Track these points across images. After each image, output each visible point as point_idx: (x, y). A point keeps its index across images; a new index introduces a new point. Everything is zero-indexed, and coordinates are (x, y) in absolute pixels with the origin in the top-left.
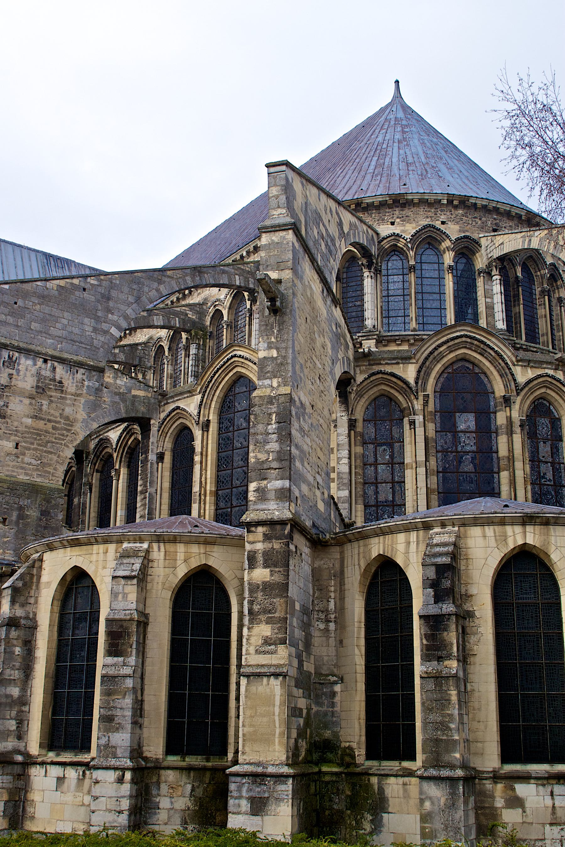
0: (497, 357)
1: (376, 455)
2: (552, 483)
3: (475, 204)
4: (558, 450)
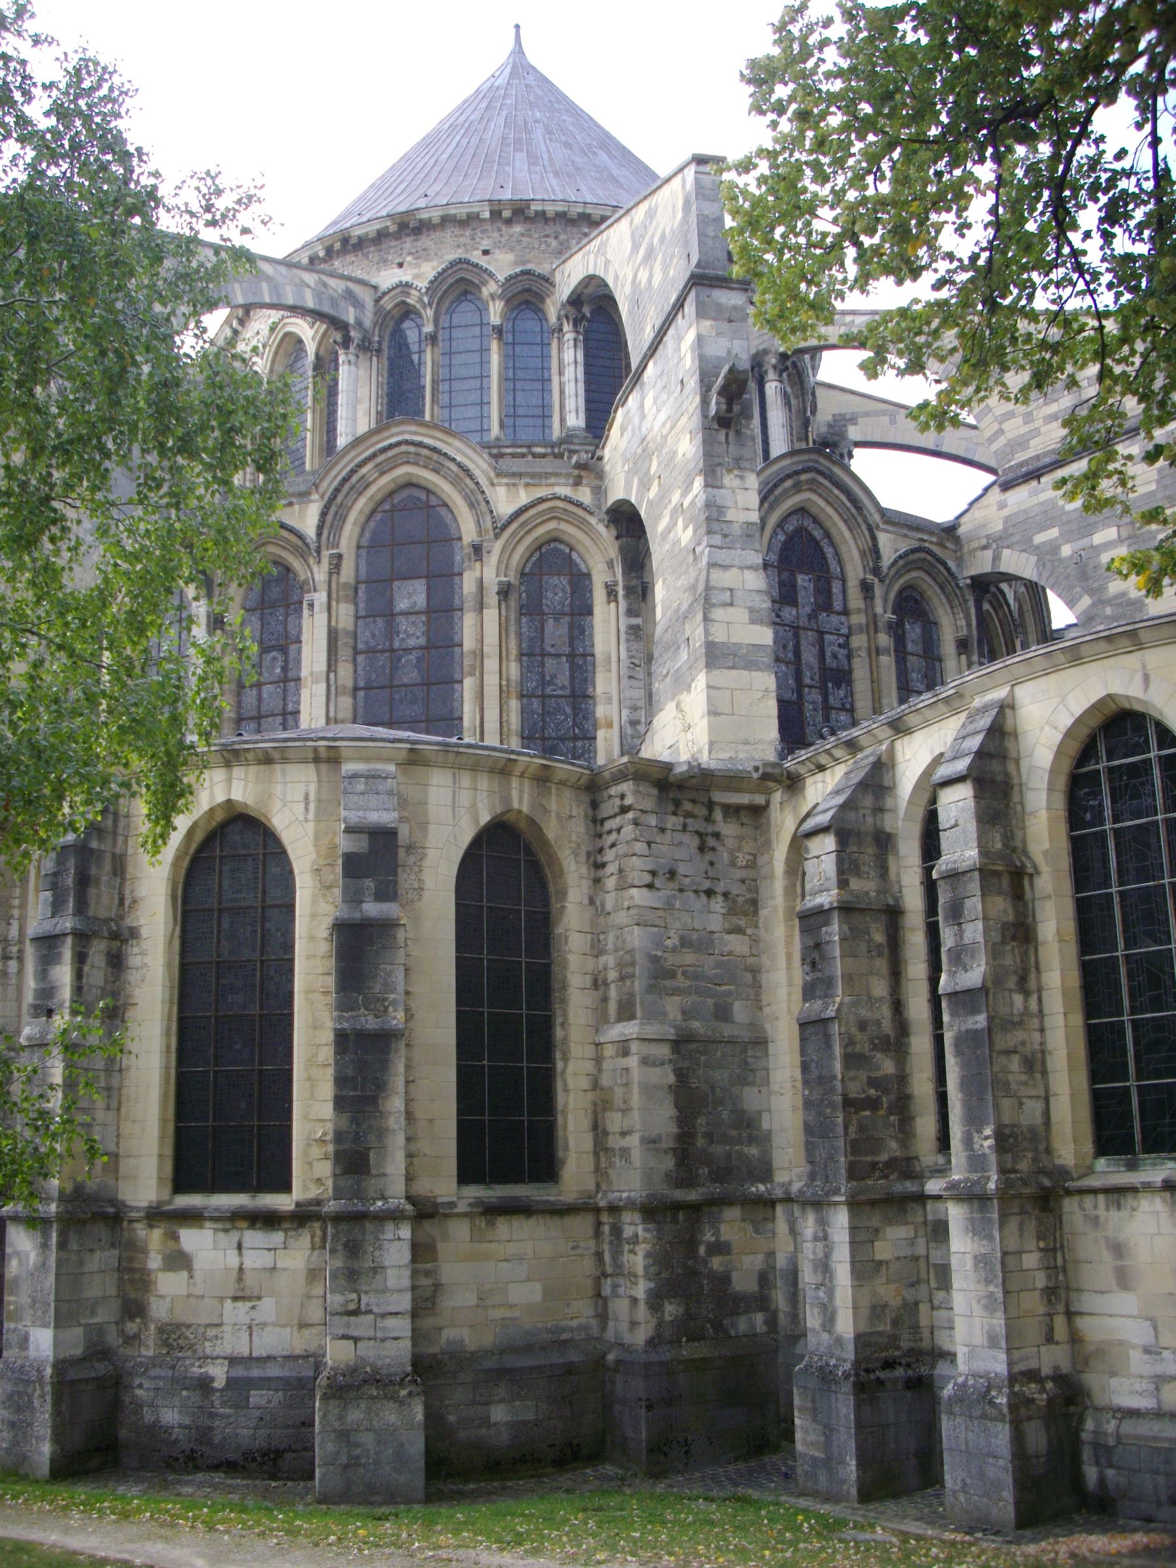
0: (462, 474)
2: (568, 692)
3: (544, 212)
4: (583, 632)
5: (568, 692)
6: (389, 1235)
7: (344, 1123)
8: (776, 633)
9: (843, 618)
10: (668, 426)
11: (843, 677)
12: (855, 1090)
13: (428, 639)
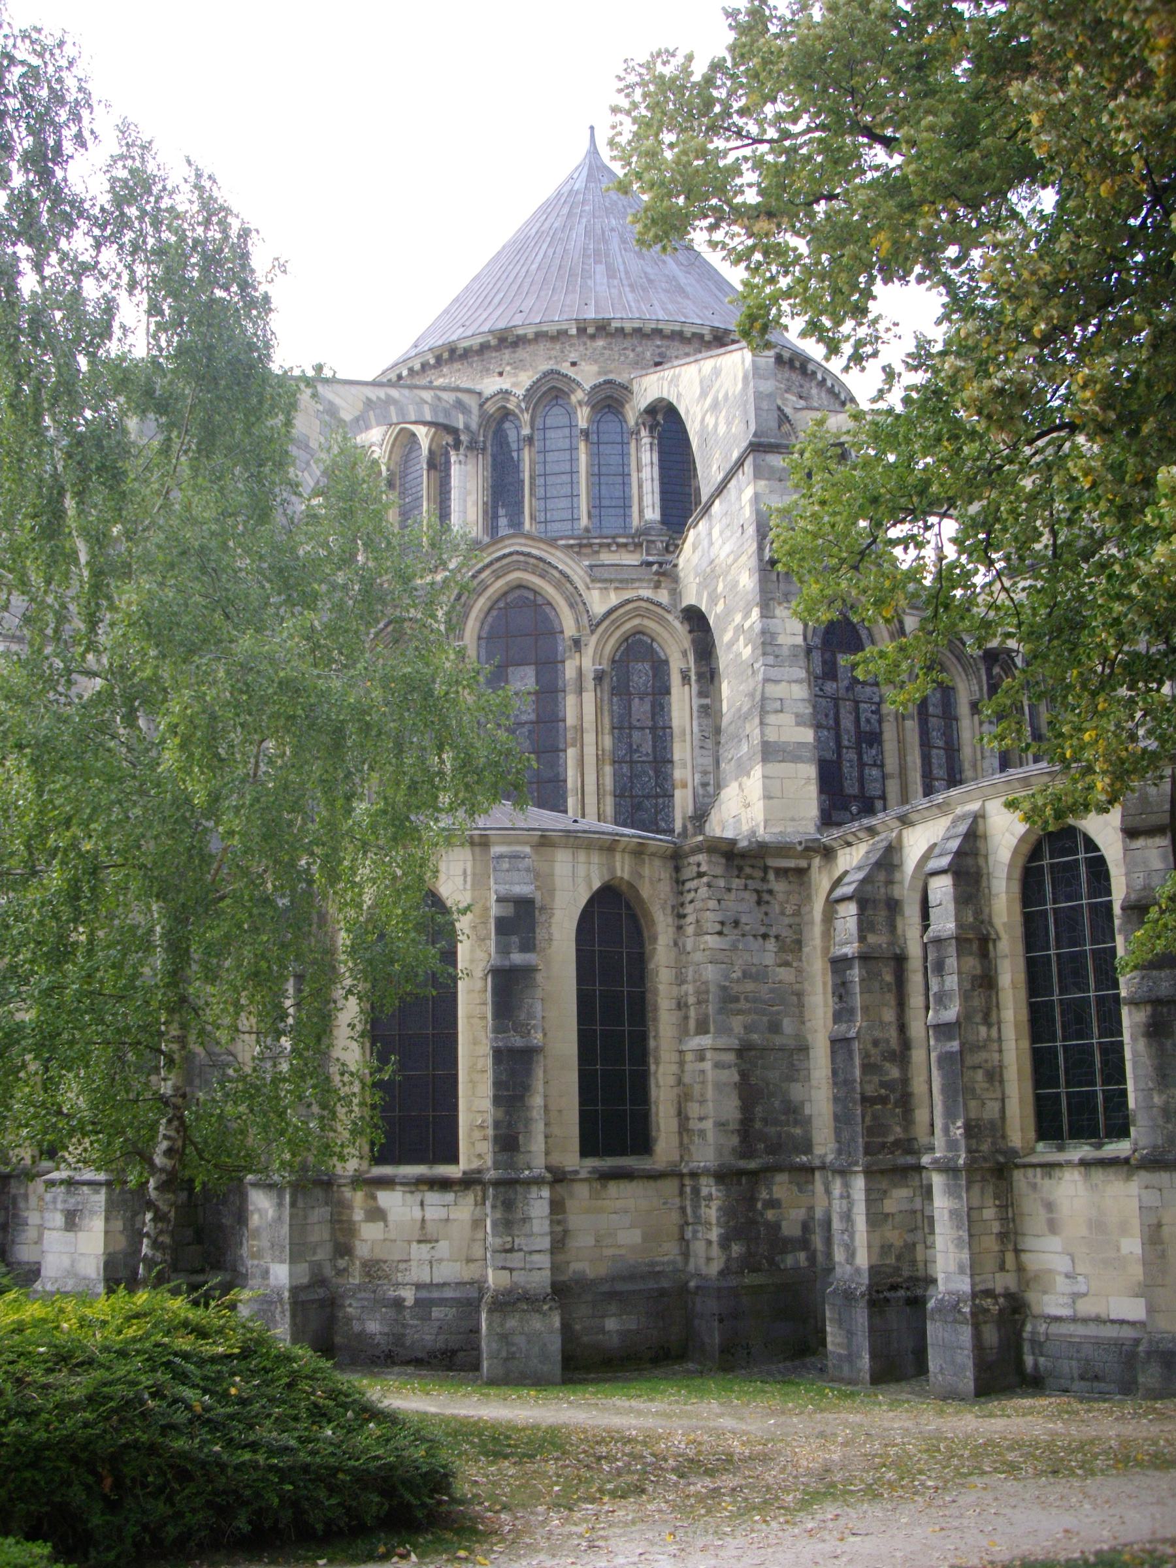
0: (563, 580)
3: (622, 329)
4: (662, 709)
5: (651, 758)
6: (534, 1195)
7: (500, 1114)
8: (816, 733)
9: (875, 689)
10: (732, 557)
11: (874, 738)
12: (870, 1091)
13: (538, 715)
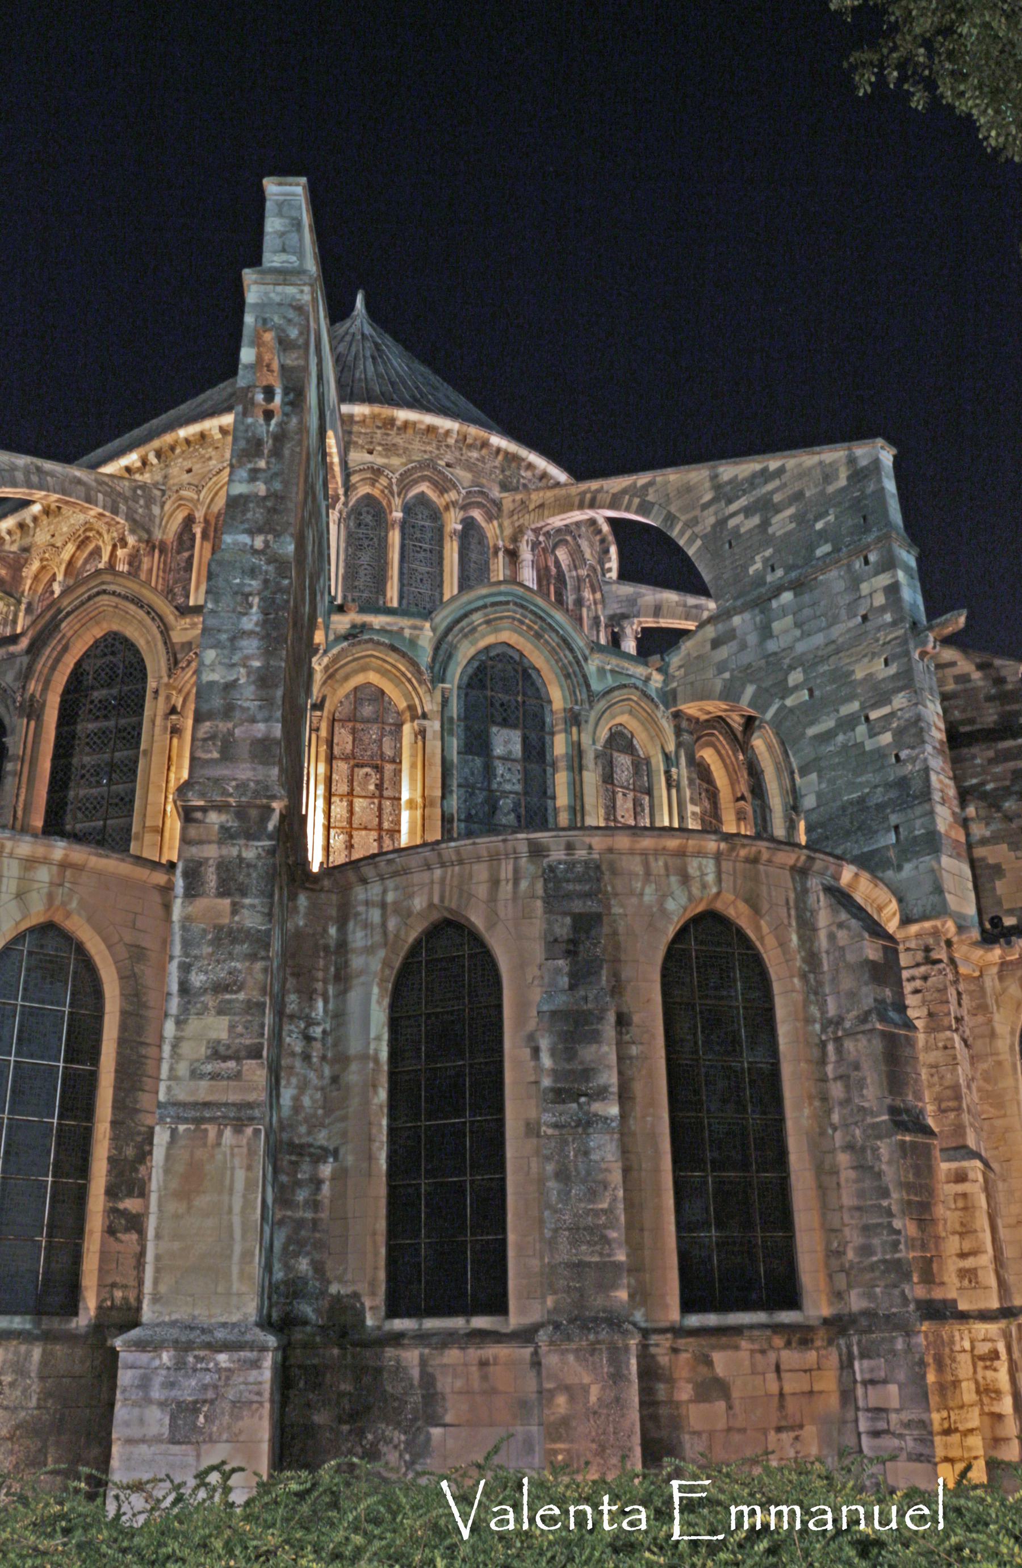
1: (351, 781)
